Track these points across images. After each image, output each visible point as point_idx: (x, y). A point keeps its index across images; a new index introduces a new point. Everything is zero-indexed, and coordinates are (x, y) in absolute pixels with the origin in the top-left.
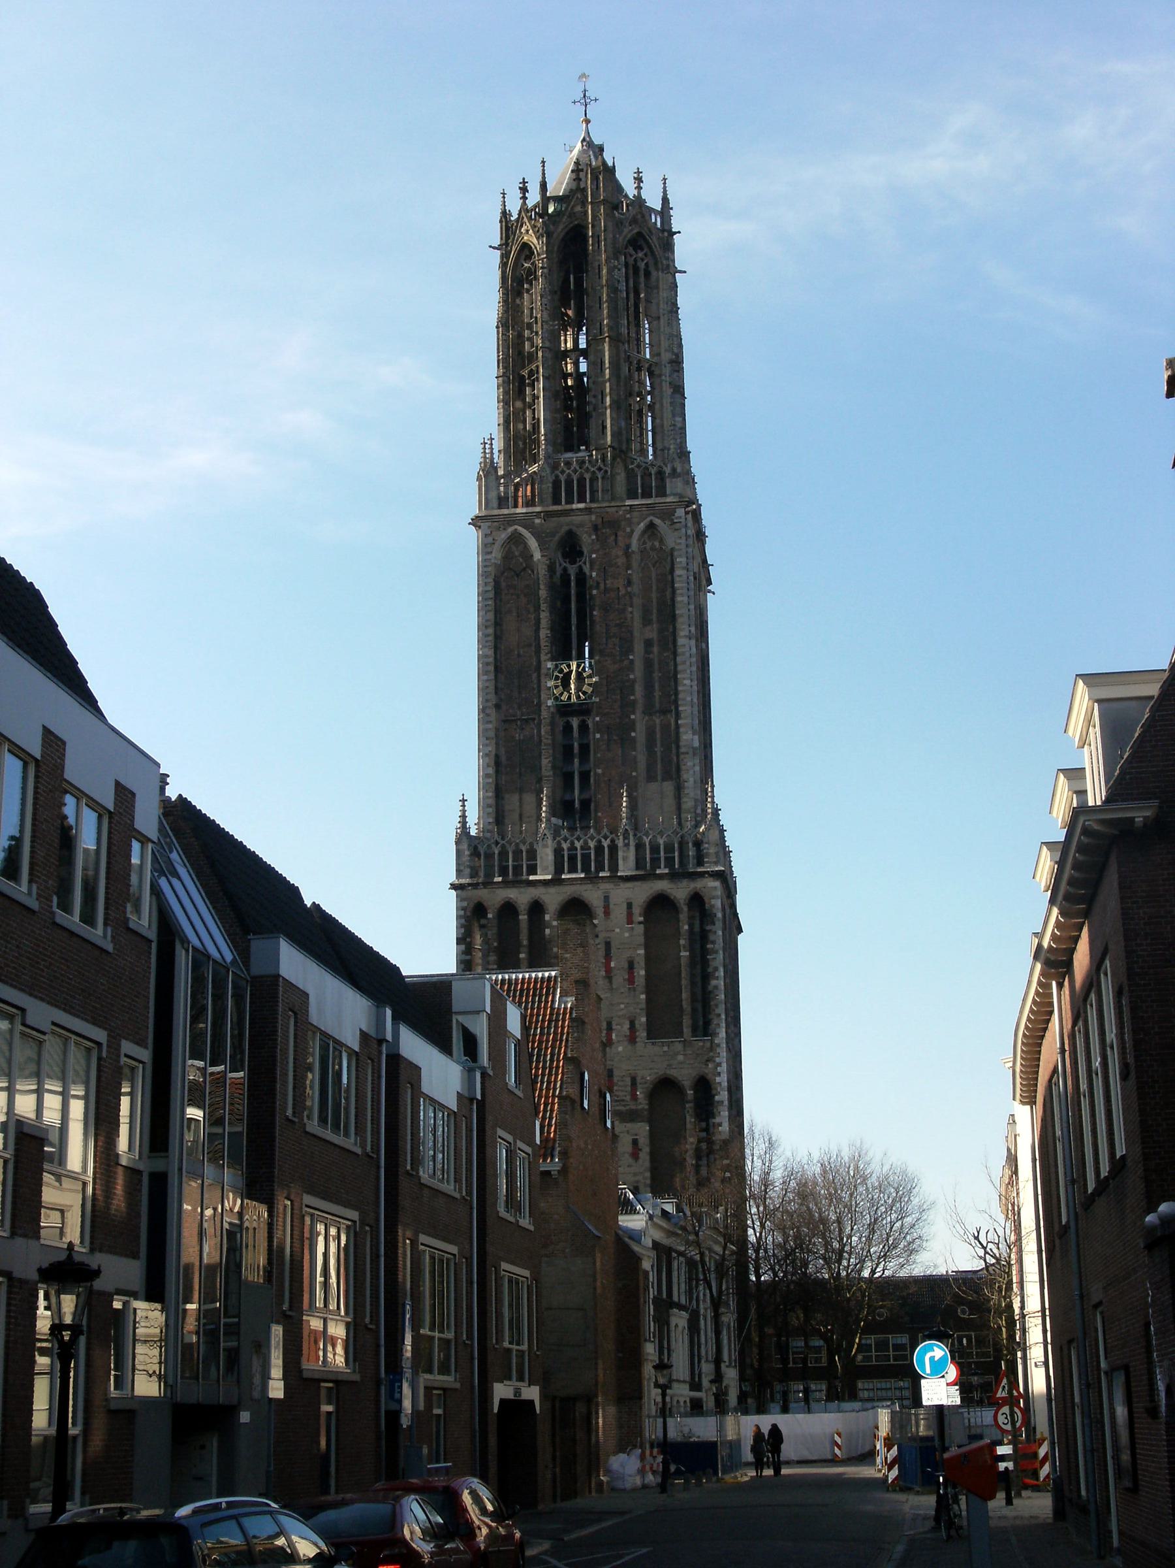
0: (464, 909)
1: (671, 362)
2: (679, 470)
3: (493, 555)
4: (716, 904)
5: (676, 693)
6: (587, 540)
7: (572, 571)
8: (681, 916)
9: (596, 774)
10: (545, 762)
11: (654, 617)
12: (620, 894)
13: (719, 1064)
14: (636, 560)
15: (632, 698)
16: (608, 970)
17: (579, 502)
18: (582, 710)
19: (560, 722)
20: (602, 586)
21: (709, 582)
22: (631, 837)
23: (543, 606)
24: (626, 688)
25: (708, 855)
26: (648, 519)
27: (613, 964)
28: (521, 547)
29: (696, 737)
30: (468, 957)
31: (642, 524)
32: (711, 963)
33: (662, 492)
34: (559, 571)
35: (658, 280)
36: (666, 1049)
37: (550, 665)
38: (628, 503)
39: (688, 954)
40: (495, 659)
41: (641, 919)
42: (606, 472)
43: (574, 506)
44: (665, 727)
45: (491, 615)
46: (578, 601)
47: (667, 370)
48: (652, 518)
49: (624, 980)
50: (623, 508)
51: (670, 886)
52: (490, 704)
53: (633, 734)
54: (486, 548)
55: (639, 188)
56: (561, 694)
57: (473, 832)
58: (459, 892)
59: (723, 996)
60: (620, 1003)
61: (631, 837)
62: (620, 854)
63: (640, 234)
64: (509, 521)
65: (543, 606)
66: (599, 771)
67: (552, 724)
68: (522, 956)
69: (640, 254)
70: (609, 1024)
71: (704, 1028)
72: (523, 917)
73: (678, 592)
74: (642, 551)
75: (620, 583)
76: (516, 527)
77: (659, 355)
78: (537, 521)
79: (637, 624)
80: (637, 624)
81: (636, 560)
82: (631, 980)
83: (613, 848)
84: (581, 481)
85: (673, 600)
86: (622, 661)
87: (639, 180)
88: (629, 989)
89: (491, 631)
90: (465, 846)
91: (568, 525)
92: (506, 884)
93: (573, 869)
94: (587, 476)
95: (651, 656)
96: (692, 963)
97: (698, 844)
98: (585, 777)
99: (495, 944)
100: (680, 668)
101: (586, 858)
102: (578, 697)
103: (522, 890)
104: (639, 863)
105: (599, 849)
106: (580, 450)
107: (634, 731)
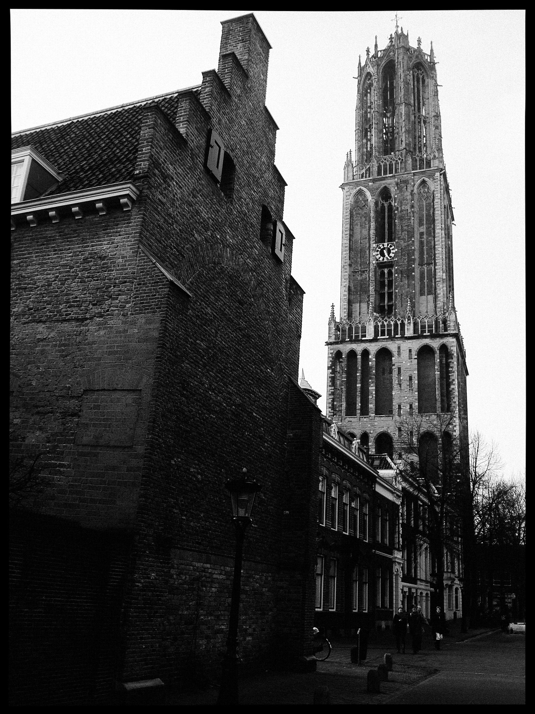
0: (331, 354)
1: (434, 116)
2: (437, 156)
3: (350, 200)
4: (454, 349)
5: (435, 255)
6: (393, 190)
7: (386, 205)
8: (436, 355)
9: (395, 292)
10: (371, 288)
11: (425, 222)
12: (406, 345)
13: (455, 426)
14: (416, 197)
15: (413, 257)
16: (400, 380)
17: (390, 174)
18: (390, 265)
20: (400, 209)
21: (453, 220)
22: (411, 319)
23: (372, 220)
24: (410, 254)
25: (449, 326)
26: (422, 178)
27: (401, 378)
28: (363, 197)
29: (444, 274)
30: (333, 375)
31: (419, 181)
32: (451, 377)
36: (427, 418)
37: (374, 245)
38: (412, 172)
39: (439, 373)
40: (350, 245)
41: (416, 357)
42: (403, 160)
43: (387, 176)
44: (429, 271)
45: (348, 226)
46: (388, 218)
48: (424, 178)
49: (407, 385)
50: (411, 174)
51: (431, 341)
52: (346, 264)
53: (413, 274)
54: (346, 197)
56: (379, 258)
57: (338, 320)
58: (329, 346)
59: (457, 393)
60: (404, 397)
61: (411, 319)
62: (406, 327)
65: (372, 220)
66: (397, 291)
67: (375, 272)
68: (358, 374)
70: (399, 406)
71: (447, 408)
72: (359, 357)
73: (436, 209)
74: (420, 193)
75: (408, 207)
76: (360, 187)
77: (428, 114)
78: (370, 184)
79: (416, 226)
80: (416, 226)
81: (416, 197)
82: (411, 385)
83: (403, 325)
84: (391, 165)
85: (434, 213)
86: (409, 241)
88: (410, 389)
90: (333, 326)
91: (384, 184)
92: (351, 341)
95: (423, 239)
96: (441, 377)
97: (445, 322)
98: (390, 295)
99: (346, 369)
100: (436, 243)
101: (389, 331)
103: (359, 344)
104: (415, 330)
105: (396, 325)
107: (414, 272)
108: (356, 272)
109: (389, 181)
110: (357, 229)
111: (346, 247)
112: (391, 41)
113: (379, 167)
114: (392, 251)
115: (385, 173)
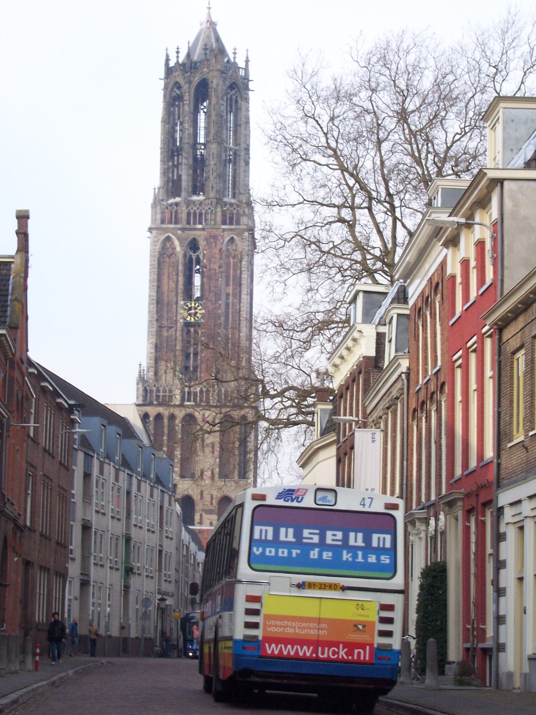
2: (247, 213)
6: (202, 244)
7: (194, 257)
18: (196, 325)
19: (185, 330)
20: (208, 267)
33: (238, 223)
35: (241, 105)
37: (182, 302)
38: (224, 227)
40: (157, 297)
42: (212, 210)
48: (233, 235)
55: (235, 58)
63: (234, 83)
64: (166, 230)
66: (203, 355)
67: (182, 330)
69: (234, 92)
72: (166, 421)
78: (179, 232)
84: (201, 214)
86: (215, 304)
87: (235, 53)
89: (155, 284)
90: (140, 386)
92: (160, 404)
93: (189, 400)
94: (204, 211)
102: (194, 319)
106: (200, 194)
109: (198, 233)
110: (165, 280)
111: (153, 300)
112: (206, 54)
113: (189, 214)
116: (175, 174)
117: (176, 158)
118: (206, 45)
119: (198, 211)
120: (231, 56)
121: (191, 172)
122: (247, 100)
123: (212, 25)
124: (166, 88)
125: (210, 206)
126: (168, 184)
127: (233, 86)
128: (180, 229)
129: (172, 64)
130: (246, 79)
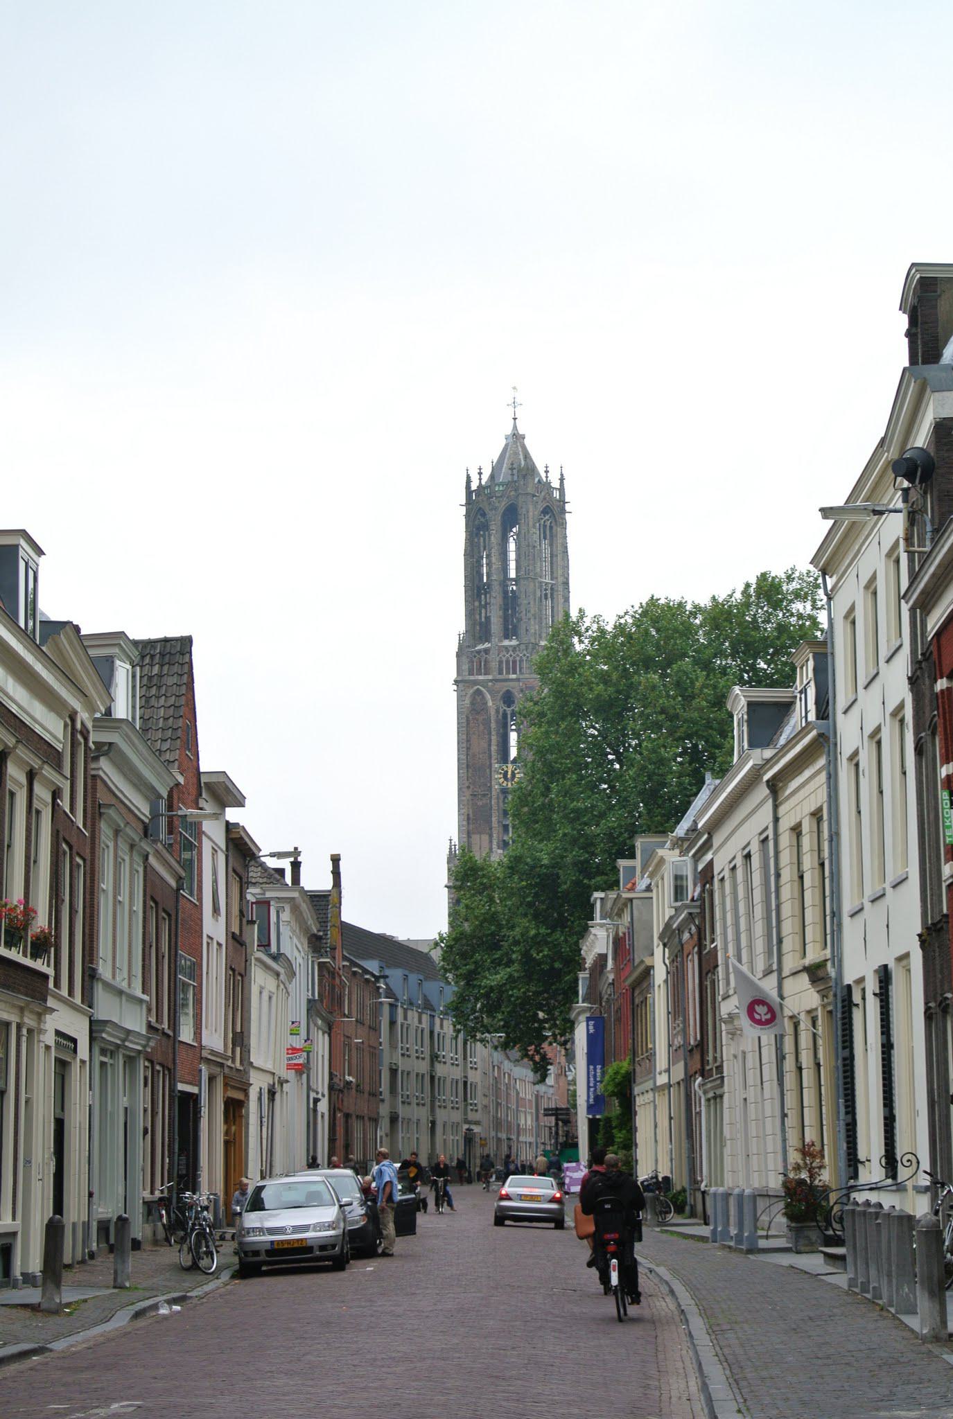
0: (452, 899)
7: (509, 711)
19: (502, 797)
34: (501, 710)
37: (496, 765)
45: (465, 737)
47: (561, 588)
55: (547, 477)
63: (547, 506)
64: (475, 683)
67: (498, 798)
69: (547, 517)
78: (490, 684)
84: (514, 662)
87: (547, 472)
94: (518, 659)
102: (512, 784)
108: (475, 795)
111: (463, 764)
112: (513, 475)
113: (501, 662)
114: (517, 776)
115: (508, 673)
116: (483, 615)
117: (483, 596)
118: (512, 464)
119: (511, 659)
120: (543, 475)
121: (501, 613)
122: (563, 525)
123: (516, 438)
124: (467, 516)
125: (525, 652)
126: (474, 628)
127: (546, 511)
128: (491, 681)
129: (474, 486)
130: (562, 501)
